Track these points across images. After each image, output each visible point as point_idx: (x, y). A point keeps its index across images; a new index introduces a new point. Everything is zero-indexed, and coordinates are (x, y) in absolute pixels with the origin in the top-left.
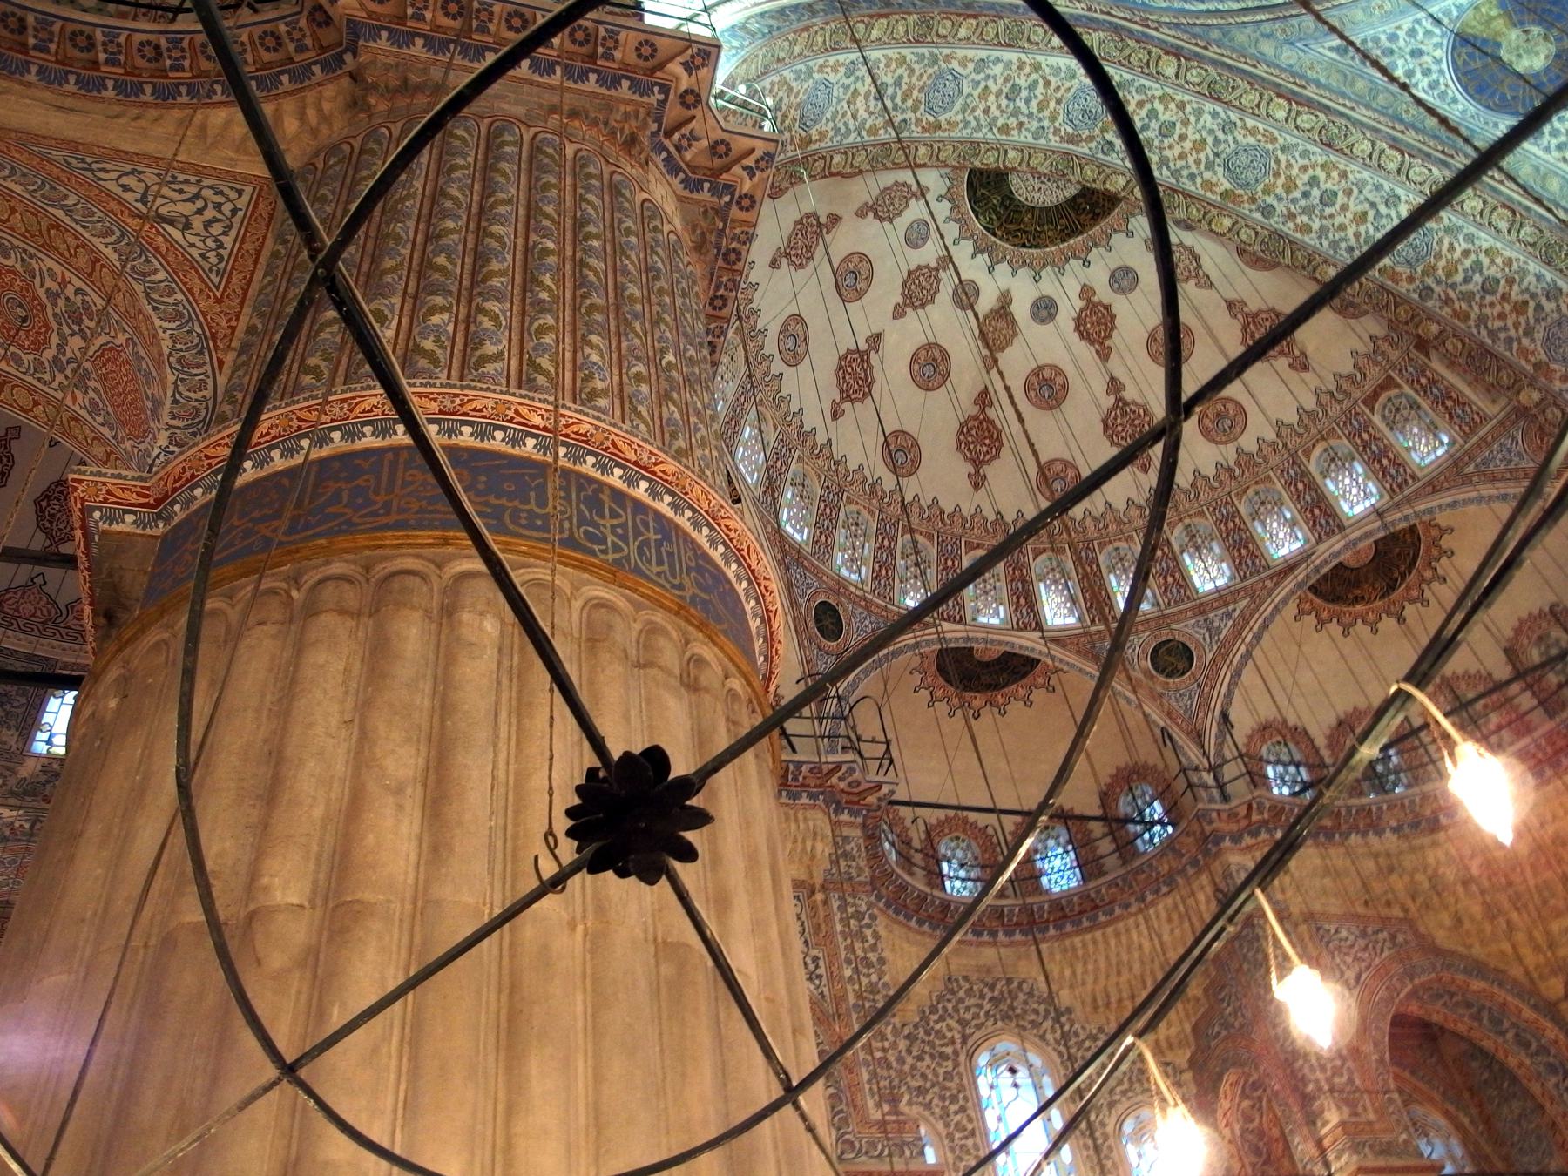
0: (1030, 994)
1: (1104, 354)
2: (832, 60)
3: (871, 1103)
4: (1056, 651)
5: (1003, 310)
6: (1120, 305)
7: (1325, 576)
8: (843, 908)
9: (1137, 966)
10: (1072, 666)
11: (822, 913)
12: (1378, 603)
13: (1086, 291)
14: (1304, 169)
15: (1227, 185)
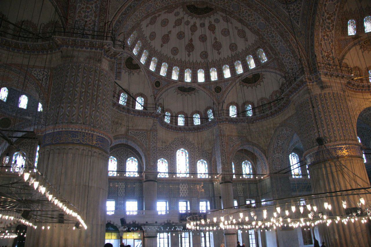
0: (188, 141)
1: (214, 33)
2: (150, 2)
3: (151, 163)
4: (199, 87)
5: (194, 25)
6: (216, 25)
7: (244, 79)
8: (152, 134)
9: (204, 138)
10: (201, 90)
11: (149, 135)
12: (253, 84)
13: (210, 22)
14: (245, 10)
15: (232, 10)
